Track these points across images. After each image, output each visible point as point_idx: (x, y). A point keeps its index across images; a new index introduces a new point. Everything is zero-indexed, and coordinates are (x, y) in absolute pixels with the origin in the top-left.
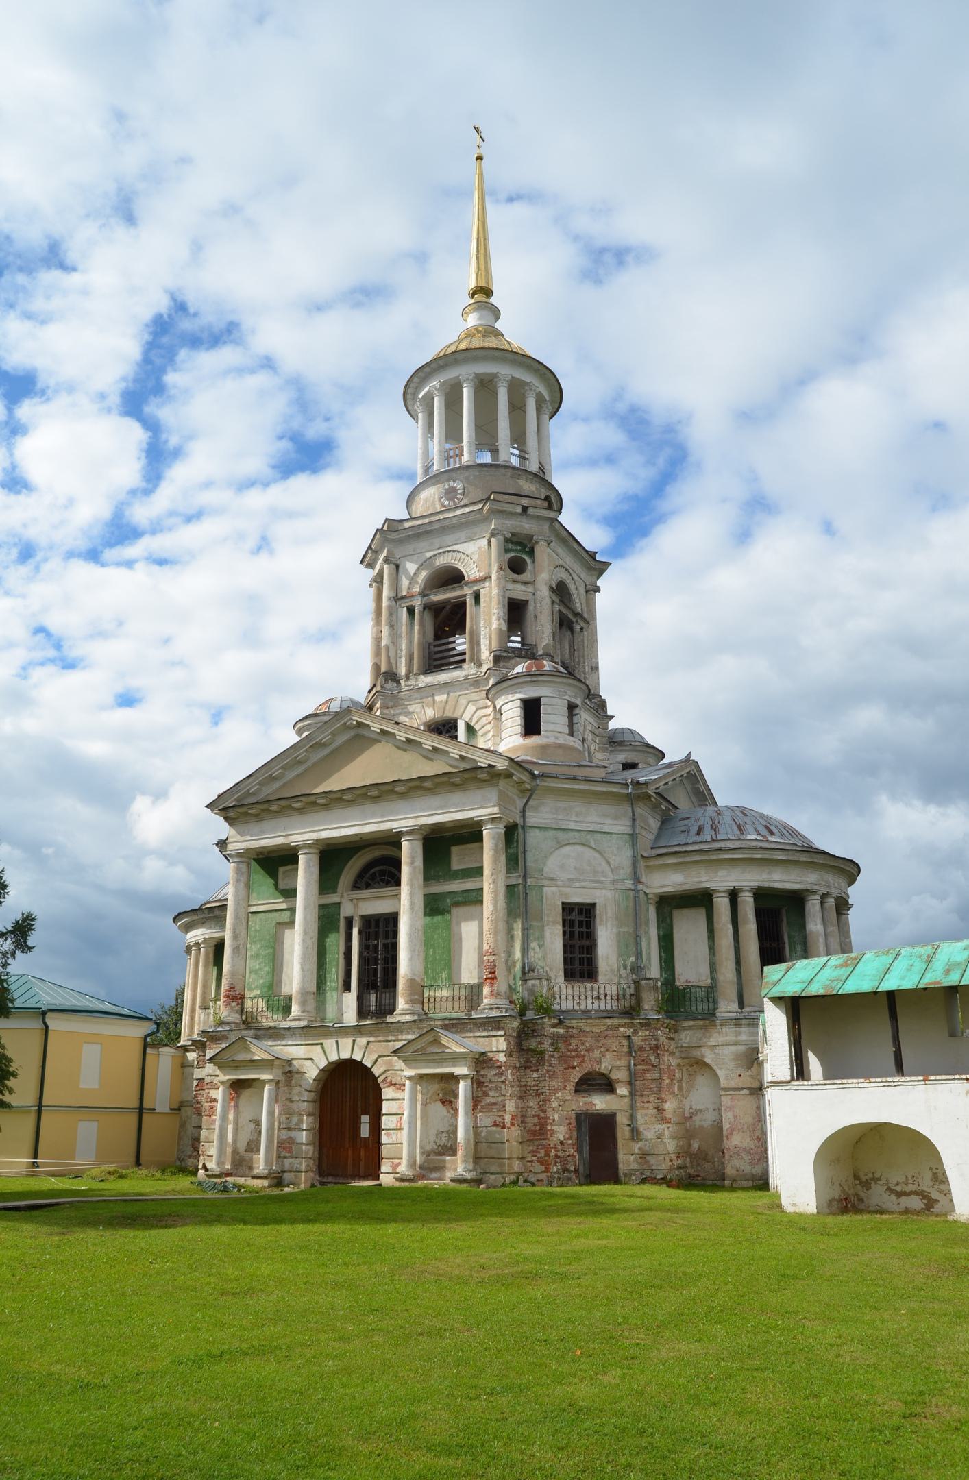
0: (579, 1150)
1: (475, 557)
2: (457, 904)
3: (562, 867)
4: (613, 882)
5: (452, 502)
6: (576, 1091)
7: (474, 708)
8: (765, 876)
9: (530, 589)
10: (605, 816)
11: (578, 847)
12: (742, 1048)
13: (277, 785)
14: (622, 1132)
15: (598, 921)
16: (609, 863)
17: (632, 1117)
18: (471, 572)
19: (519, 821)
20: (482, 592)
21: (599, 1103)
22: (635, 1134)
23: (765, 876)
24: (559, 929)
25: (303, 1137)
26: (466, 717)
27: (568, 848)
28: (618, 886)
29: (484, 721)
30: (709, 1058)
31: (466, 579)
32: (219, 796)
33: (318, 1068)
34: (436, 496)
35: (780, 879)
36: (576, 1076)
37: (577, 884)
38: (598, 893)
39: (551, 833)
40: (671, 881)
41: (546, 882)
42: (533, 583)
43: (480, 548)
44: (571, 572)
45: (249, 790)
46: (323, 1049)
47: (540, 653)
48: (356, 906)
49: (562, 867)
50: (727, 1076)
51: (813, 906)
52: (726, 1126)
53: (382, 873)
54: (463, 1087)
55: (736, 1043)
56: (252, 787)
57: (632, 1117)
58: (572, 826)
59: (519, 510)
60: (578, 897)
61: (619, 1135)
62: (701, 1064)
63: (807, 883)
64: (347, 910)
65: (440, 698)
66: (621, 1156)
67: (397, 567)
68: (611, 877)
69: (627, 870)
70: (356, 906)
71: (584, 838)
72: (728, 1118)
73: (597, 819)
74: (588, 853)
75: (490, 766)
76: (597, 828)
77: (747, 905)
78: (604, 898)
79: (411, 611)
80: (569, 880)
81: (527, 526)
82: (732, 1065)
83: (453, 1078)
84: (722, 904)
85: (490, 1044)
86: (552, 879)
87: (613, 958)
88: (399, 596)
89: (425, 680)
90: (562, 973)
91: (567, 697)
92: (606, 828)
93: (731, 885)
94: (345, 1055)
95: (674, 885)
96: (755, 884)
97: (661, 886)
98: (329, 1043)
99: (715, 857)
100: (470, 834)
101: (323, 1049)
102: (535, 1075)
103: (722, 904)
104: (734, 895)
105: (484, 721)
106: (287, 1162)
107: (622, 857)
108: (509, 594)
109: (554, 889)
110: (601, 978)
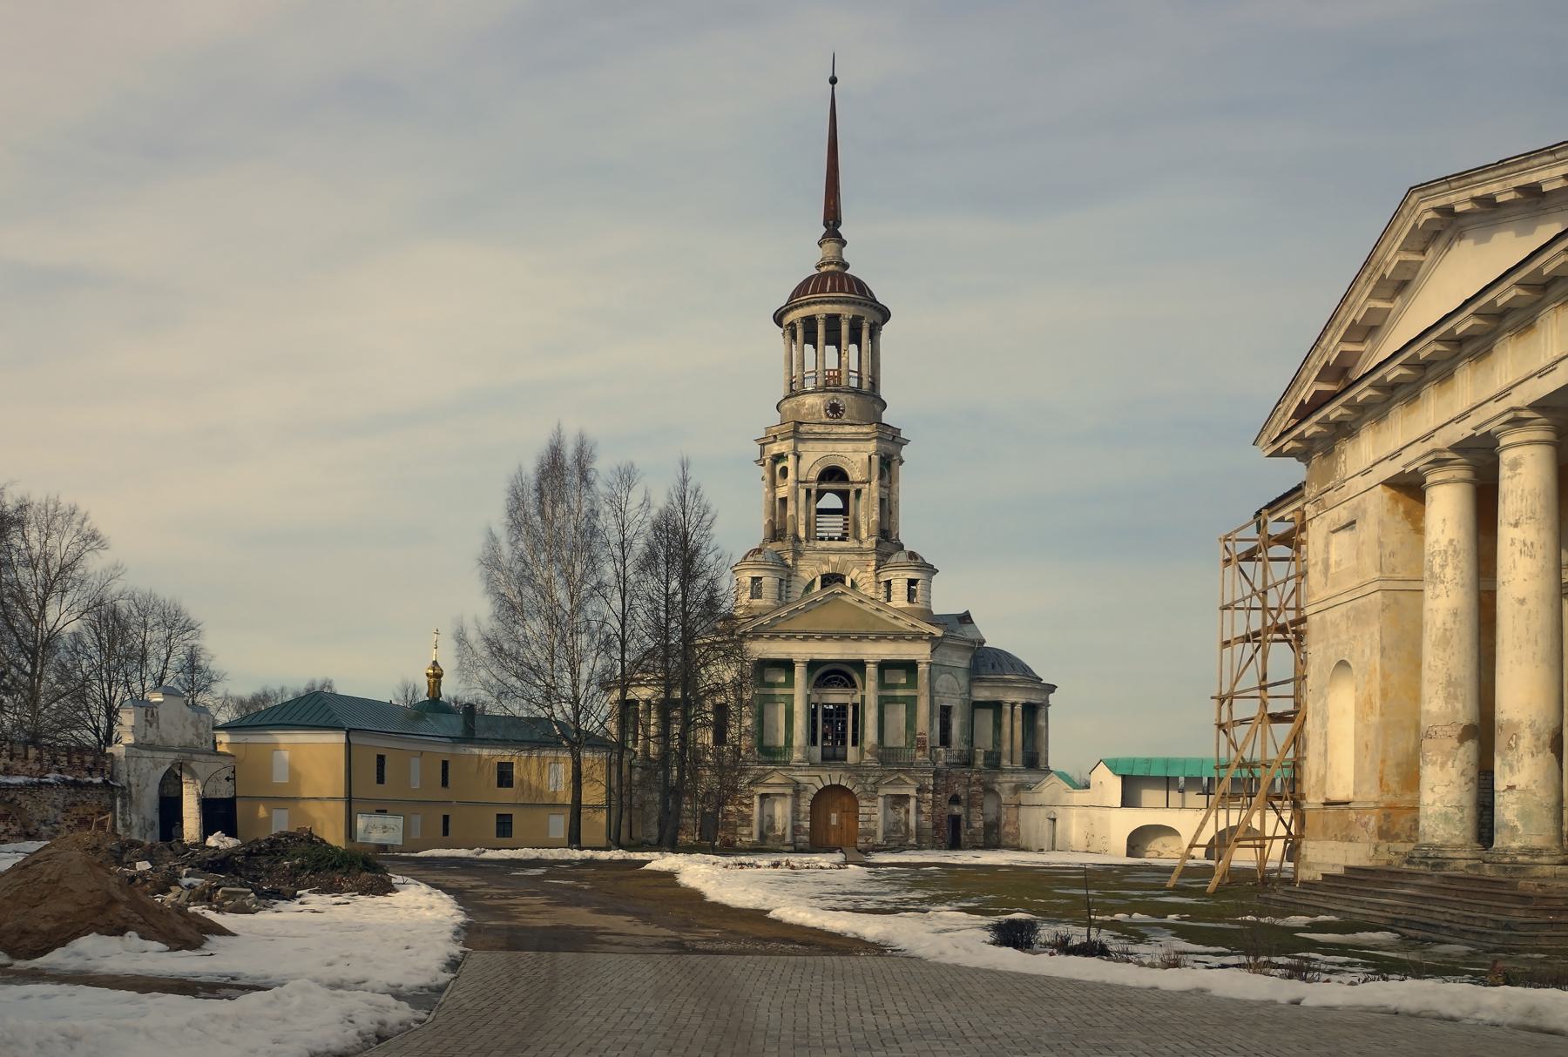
0: (948, 832)
1: (859, 465)
2: (888, 703)
3: (941, 686)
5: (835, 416)
6: (949, 804)
7: (858, 571)
10: (959, 658)
12: (1013, 784)
14: (963, 824)
15: (952, 715)
17: (968, 817)
18: (855, 474)
21: (957, 810)
22: (969, 826)
26: (853, 575)
27: (943, 676)
28: (962, 696)
29: (864, 581)
30: (997, 788)
31: (851, 480)
34: (822, 407)
35: (1034, 698)
36: (949, 796)
39: (938, 667)
40: (982, 694)
42: (889, 488)
43: (862, 459)
48: (820, 698)
49: (941, 686)
50: (1006, 798)
52: (1003, 822)
53: (836, 679)
54: (913, 802)
55: (1013, 782)
57: (968, 817)
61: (962, 826)
62: (993, 791)
64: (815, 699)
65: (834, 558)
66: (962, 836)
67: (798, 458)
69: (965, 689)
70: (820, 698)
72: (1004, 818)
73: (955, 659)
74: (951, 678)
77: (1018, 708)
78: (955, 702)
79: (808, 492)
80: (945, 693)
81: (891, 448)
82: (1008, 792)
83: (907, 797)
85: (924, 780)
86: (938, 692)
87: (958, 736)
88: (802, 478)
90: (939, 743)
93: (1013, 700)
94: (835, 782)
95: (986, 697)
96: (1024, 701)
98: (824, 775)
100: (910, 667)
102: (939, 796)
104: (1013, 705)
105: (864, 581)
106: (798, 837)
107: (963, 681)
110: (953, 747)
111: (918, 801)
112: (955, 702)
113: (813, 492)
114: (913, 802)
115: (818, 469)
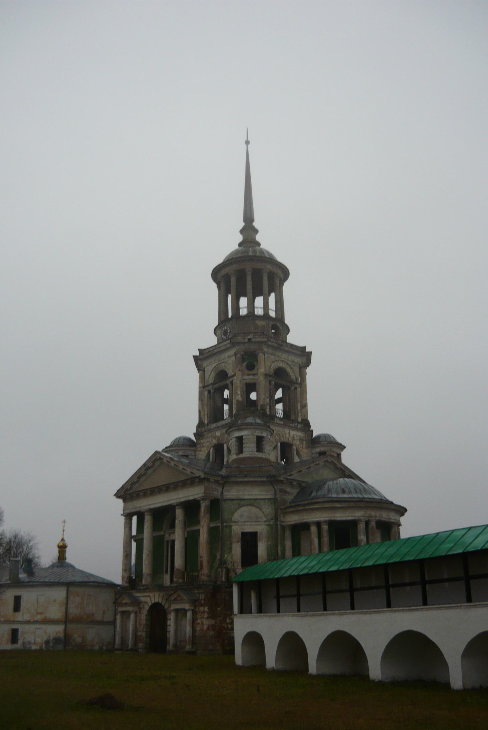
3: (241, 516)
4: (265, 522)
8: (332, 515)
9: (256, 377)
11: (250, 508)
13: (137, 485)
16: (263, 513)
19: (219, 497)
20: (234, 382)
23: (332, 515)
24: (239, 544)
25: (144, 635)
27: (243, 509)
32: (118, 491)
33: (149, 606)
37: (248, 524)
38: (258, 527)
39: (236, 502)
41: (233, 524)
42: (257, 374)
43: (233, 361)
44: (286, 361)
45: (127, 488)
46: (150, 598)
47: (259, 408)
51: (361, 526)
54: (189, 614)
56: (128, 487)
58: (246, 497)
59: (246, 340)
60: (248, 529)
63: (355, 516)
65: (218, 433)
67: (204, 371)
68: (265, 519)
71: (253, 502)
75: (199, 476)
76: (258, 497)
77: (325, 527)
78: (261, 529)
79: (209, 392)
80: (244, 522)
83: (185, 611)
84: (314, 529)
86: (235, 522)
88: (206, 384)
89: (214, 426)
90: (240, 564)
91: (256, 434)
92: (262, 497)
97: (290, 522)
99: (307, 508)
101: (150, 598)
102: (219, 609)
103: (314, 529)
104: (318, 524)
108: (245, 381)
109: (238, 527)
111: (194, 612)
112: (261, 529)
113: (212, 391)
114: (189, 614)
115: (213, 374)
